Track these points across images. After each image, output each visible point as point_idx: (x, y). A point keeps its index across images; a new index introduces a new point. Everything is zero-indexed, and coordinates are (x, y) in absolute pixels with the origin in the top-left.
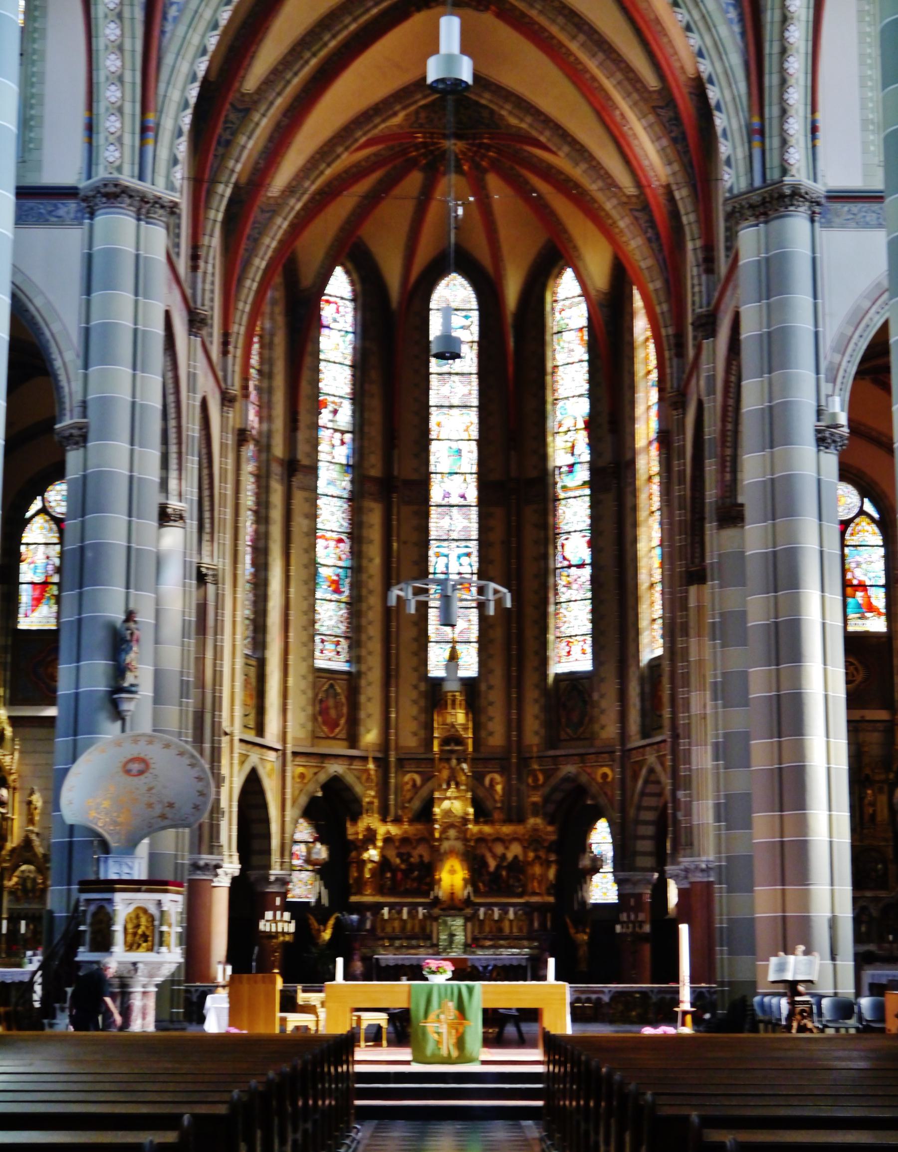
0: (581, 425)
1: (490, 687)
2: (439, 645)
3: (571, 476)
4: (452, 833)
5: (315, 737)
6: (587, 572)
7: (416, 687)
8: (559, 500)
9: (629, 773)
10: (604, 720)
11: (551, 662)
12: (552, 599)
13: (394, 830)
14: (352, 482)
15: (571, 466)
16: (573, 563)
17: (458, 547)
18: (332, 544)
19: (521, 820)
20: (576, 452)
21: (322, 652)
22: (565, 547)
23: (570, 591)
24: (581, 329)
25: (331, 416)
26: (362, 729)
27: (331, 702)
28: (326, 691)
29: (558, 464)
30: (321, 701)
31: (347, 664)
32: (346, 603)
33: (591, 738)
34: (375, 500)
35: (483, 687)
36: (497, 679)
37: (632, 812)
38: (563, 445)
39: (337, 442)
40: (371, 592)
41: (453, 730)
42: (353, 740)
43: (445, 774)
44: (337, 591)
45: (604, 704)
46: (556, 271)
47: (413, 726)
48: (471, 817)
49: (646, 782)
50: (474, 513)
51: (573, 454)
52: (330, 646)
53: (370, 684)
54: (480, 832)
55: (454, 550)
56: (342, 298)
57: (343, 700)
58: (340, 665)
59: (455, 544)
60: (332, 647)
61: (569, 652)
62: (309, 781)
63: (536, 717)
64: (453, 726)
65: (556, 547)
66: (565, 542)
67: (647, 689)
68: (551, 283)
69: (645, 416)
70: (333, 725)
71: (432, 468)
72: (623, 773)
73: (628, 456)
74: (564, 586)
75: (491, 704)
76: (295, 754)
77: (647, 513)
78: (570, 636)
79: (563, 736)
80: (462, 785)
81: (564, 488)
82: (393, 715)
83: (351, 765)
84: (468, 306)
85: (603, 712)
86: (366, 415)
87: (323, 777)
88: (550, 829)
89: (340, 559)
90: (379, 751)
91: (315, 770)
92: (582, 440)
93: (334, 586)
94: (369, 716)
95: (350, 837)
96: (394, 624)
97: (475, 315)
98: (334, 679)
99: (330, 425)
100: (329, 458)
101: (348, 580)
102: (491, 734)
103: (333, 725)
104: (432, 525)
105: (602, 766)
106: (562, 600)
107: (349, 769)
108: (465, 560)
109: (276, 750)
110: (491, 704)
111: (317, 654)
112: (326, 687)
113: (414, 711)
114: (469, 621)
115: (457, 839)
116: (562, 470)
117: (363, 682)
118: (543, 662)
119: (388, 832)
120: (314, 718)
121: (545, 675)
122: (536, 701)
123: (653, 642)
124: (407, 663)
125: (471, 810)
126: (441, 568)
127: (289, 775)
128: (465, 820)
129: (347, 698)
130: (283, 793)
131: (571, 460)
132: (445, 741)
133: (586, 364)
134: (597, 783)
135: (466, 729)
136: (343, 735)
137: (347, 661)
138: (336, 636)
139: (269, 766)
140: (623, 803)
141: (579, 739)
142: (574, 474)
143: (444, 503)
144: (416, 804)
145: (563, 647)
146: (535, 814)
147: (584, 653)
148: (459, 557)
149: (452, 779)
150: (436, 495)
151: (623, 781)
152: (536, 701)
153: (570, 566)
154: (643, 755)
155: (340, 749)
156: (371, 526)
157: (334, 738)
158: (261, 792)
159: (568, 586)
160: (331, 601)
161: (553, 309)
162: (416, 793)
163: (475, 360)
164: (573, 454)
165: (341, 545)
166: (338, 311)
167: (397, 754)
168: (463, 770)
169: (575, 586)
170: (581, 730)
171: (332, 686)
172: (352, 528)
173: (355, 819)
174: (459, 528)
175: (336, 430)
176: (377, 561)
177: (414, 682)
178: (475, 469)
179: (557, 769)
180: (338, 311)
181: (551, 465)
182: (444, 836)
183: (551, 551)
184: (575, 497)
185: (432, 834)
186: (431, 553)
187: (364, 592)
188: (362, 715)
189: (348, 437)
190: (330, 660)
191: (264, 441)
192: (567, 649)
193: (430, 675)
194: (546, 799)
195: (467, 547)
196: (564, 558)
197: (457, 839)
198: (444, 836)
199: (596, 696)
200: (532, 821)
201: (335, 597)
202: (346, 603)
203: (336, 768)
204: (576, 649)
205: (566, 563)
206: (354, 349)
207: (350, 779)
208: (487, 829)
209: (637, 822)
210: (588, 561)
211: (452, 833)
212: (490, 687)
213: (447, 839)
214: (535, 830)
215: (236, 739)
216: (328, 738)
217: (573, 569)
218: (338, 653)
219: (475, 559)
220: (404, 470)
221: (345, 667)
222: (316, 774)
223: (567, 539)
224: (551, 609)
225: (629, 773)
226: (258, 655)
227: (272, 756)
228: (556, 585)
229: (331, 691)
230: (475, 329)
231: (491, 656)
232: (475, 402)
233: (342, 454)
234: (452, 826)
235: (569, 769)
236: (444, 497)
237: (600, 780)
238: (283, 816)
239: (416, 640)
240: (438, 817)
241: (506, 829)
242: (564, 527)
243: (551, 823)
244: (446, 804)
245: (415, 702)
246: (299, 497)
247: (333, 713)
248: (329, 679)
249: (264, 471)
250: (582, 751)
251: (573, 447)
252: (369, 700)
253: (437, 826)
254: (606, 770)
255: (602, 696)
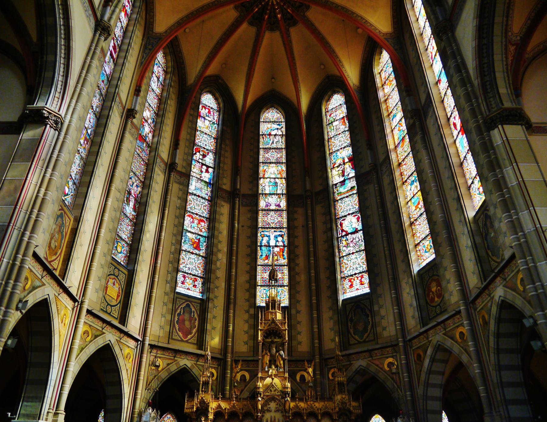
0: (346, 160)
1: (298, 312)
2: (262, 288)
3: (343, 187)
4: (273, 405)
5: (170, 336)
6: (360, 234)
7: (247, 311)
8: (337, 201)
9: (412, 358)
10: (384, 323)
11: (340, 292)
12: (337, 254)
13: (224, 405)
14: (212, 192)
15: (344, 181)
16: (349, 232)
17: (275, 231)
18: (196, 221)
19: (331, 399)
20: (346, 174)
21: (183, 283)
22: (344, 225)
23: (349, 248)
24: (343, 118)
25: (201, 157)
26: (208, 338)
27: (187, 316)
28: (184, 308)
29: (335, 183)
30: (179, 315)
31: (201, 295)
32: (202, 257)
33: (376, 337)
34: (225, 201)
35: (293, 312)
36: (303, 306)
37: (420, 391)
38: (337, 173)
39: (204, 170)
40: (219, 251)
41: (273, 324)
42: (201, 343)
43: (267, 359)
44: (198, 248)
45: (383, 312)
46: (326, 98)
47: (245, 338)
48: (289, 390)
49: (433, 360)
50: (285, 214)
51: (343, 176)
52: (189, 281)
53: (215, 307)
54: (297, 406)
55: (272, 234)
56: (212, 108)
57: (196, 316)
58: (196, 293)
59: (273, 230)
60: (191, 281)
61: (351, 286)
62: (163, 369)
63: (331, 329)
64: (273, 321)
65: (337, 226)
66: (342, 222)
67: (420, 291)
68: (324, 103)
69: (391, 134)
70: (187, 333)
71: (260, 192)
72: (407, 359)
73: (382, 158)
74: (345, 246)
75: (299, 323)
76: (152, 346)
77: (401, 182)
78: (352, 276)
79: (352, 341)
80: (281, 368)
81: (340, 194)
82: (231, 329)
83: (197, 361)
84: (280, 120)
85: (383, 318)
86: (222, 159)
87: (174, 368)
88: (354, 404)
89: (201, 231)
90: (221, 354)
91: (169, 362)
92: (348, 169)
93: (195, 245)
94: (214, 328)
95: (186, 411)
96: (234, 270)
97: (284, 124)
98: (191, 302)
99: (200, 161)
100: (199, 177)
101: (205, 244)
102: (300, 343)
103: (187, 333)
104: (260, 220)
105: (387, 358)
106: (344, 255)
107: (196, 364)
108: (280, 239)
109: (136, 340)
110: (299, 323)
111: (180, 284)
112: (184, 305)
113: (246, 327)
114: (283, 273)
115: (277, 411)
116: (338, 185)
117: (210, 305)
118: (335, 292)
119: (219, 406)
120: (171, 323)
121: (337, 300)
122: (331, 318)
123: (418, 259)
124: (241, 296)
125: (289, 385)
126: (264, 242)
127: (144, 360)
128: (284, 393)
129: (199, 316)
130: (138, 375)
131: (342, 179)
132: (268, 334)
133: (347, 133)
134: (385, 371)
135: (283, 324)
136: (193, 341)
137: (201, 293)
138: (194, 275)
139: (126, 351)
140: (411, 382)
141: (365, 342)
142: (346, 185)
143: (267, 208)
144: (246, 394)
145: (347, 284)
146: (341, 392)
147: (362, 284)
148: (276, 237)
149: (273, 362)
150: (262, 204)
151: (408, 365)
152: (331, 318)
153: (347, 234)
154: (428, 338)
155: (192, 349)
156: (222, 214)
157: (187, 342)
158: (116, 371)
159: (347, 246)
160: (192, 253)
161: (326, 115)
162: (246, 386)
163: (284, 143)
164: (343, 176)
165: (203, 224)
166: (209, 112)
167: (232, 357)
168: (281, 356)
169: (351, 245)
170: (366, 335)
171: (188, 306)
172: (210, 216)
173: (192, 397)
174: (276, 221)
175: (203, 164)
176: (225, 232)
177: (247, 308)
178: (284, 192)
179: (351, 364)
180: (209, 112)
181: (331, 183)
182: (265, 408)
183: (334, 227)
184: (347, 197)
185: (257, 406)
186: (259, 234)
187: (215, 250)
188: (209, 327)
189: (210, 170)
190: (188, 289)
191: (154, 146)
192: (350, 284)
193: (258, 304)
194: (350, 380)
195: (281, 231)
196: (343, 231)
197: (277, 411)
198: (265, 408)
199: (376, 308)
200: (339, 397)
201: (196, 251)
202: (202, 257)
203: (185, 362)
204: (356, 282)
205: (344, 233)
206: (218, 131)
207: (196, 371)
208: (302, 405)
209: (426, 398)
210: (360, 227)
211: (273, 405)
212: (298, 312)
213: (269, 411)
214: (343, 403)
215: (86, 307)
216: (182, 341)
217: (350, 235)
218: (195, 286)
219: (285, 238)
220: (244, 188)
221: (199, 296)
222: (168, 364)
223: (344, 220)
224: (337, 260)
225: (412, 358)
226: (130, 267)
227: (132, 343)
228: (339, 247)
229: (187, 309)
230: (284, 130)
231: (298, 292)
232: (284, 161)
233: (207, 177)
234: (272, 399)
235: (360, 363)
236: (267, 206)
237: (387, 369)
238: (136, 394)
239: (248, 282)
240: (261, 390)
241: (318, 405)
242: (341, 214)
243: (356, 399)
244: (268, 381)
245: (247, 321)
246: (175, 188)
247: (187, 323)
248: (187, 301)
249: (151, 162)
250: (370, 348)
251: (343, 172)
252: (214, 317)
253: (260, 399)
254: (391, 360)
255: (381, 307)
